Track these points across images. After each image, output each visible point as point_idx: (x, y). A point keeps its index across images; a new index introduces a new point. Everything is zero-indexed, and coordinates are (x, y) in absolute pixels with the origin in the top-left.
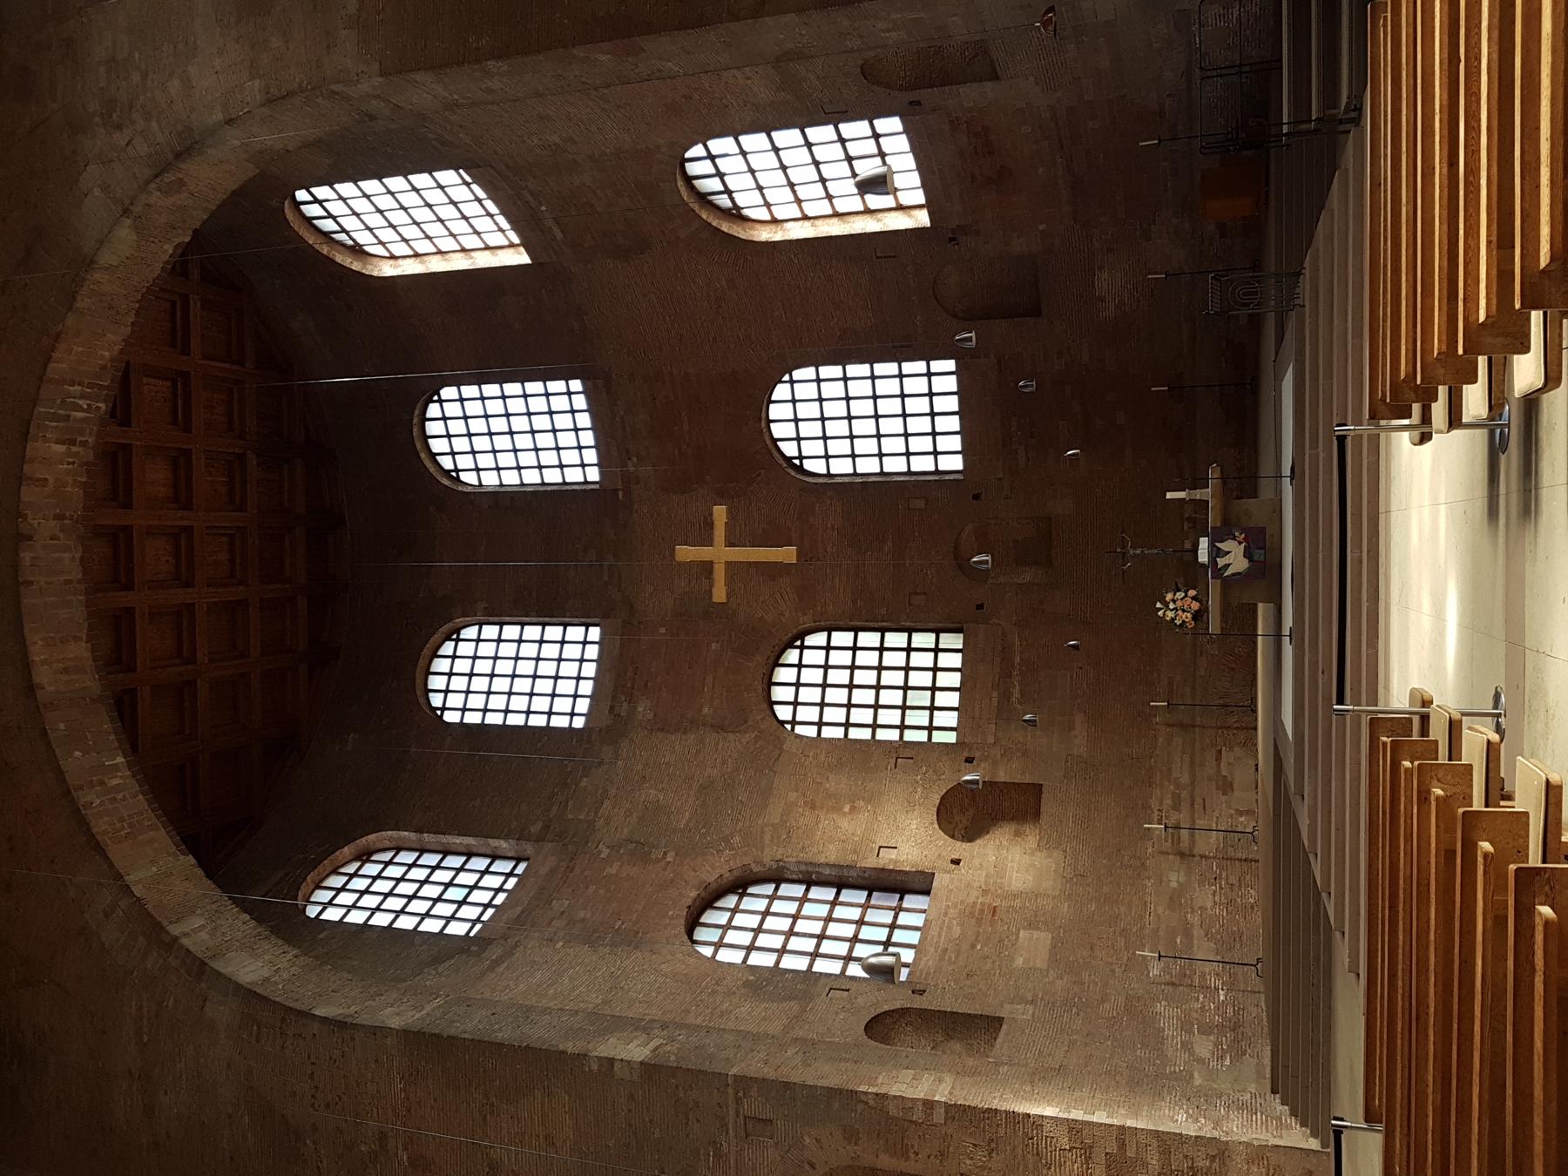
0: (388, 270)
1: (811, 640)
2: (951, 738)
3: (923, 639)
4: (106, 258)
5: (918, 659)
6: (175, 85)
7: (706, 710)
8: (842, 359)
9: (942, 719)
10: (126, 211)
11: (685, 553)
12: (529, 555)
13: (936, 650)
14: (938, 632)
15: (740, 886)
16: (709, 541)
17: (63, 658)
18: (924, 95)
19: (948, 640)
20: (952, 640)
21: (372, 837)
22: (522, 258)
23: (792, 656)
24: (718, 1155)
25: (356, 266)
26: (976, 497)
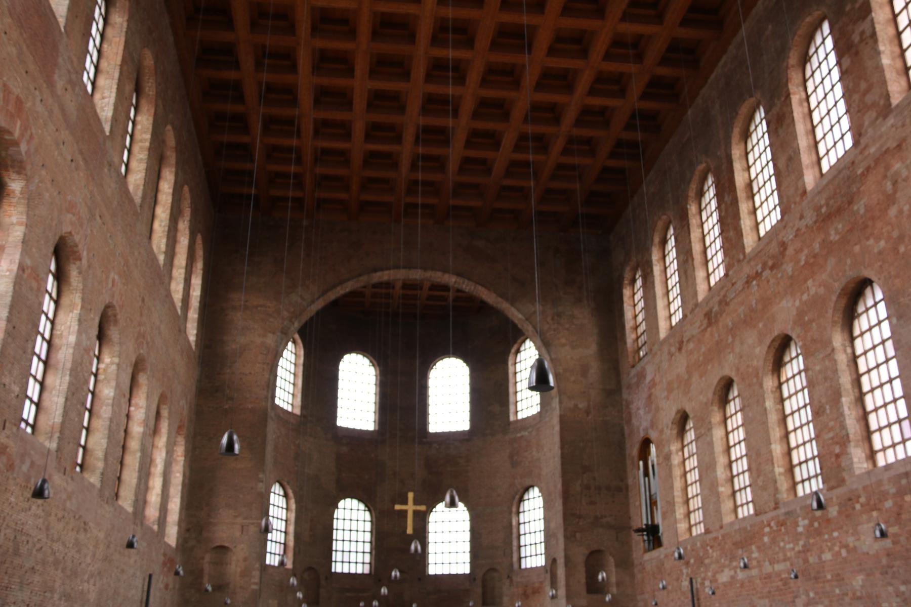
0: (510, 362)
1: (367, 513)
2: (333, 570)
3: (367, 558)
4: (513, 309)
5: (360, 555)
6: (563, 341)
7: (344, 475)
8: (472, 530)
9: (339, 565)
10: (527, 319)
11: (411, 495)
12: (402, 398)
13: (363, 563)
14: (370, 563)
15: (286, 495)
16: (416, 503)
17: (385, 276)
18: (548, 575)
19: (367, 567)
20: (367, 571)
21: (301, 345)
22: (512, 418)
23: (362, 506)
24: (236, 517)
25: (513, 351)
26: (419, 579)
